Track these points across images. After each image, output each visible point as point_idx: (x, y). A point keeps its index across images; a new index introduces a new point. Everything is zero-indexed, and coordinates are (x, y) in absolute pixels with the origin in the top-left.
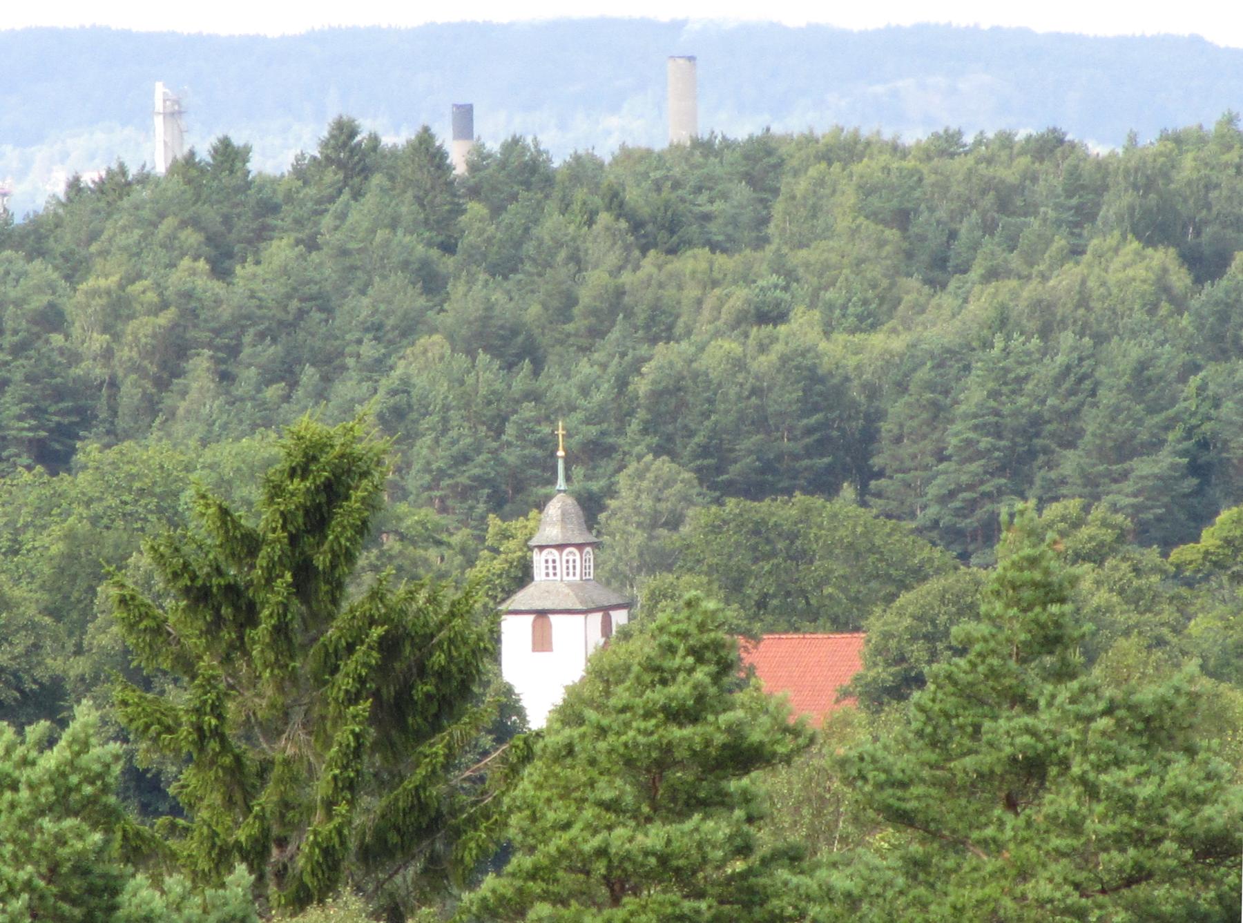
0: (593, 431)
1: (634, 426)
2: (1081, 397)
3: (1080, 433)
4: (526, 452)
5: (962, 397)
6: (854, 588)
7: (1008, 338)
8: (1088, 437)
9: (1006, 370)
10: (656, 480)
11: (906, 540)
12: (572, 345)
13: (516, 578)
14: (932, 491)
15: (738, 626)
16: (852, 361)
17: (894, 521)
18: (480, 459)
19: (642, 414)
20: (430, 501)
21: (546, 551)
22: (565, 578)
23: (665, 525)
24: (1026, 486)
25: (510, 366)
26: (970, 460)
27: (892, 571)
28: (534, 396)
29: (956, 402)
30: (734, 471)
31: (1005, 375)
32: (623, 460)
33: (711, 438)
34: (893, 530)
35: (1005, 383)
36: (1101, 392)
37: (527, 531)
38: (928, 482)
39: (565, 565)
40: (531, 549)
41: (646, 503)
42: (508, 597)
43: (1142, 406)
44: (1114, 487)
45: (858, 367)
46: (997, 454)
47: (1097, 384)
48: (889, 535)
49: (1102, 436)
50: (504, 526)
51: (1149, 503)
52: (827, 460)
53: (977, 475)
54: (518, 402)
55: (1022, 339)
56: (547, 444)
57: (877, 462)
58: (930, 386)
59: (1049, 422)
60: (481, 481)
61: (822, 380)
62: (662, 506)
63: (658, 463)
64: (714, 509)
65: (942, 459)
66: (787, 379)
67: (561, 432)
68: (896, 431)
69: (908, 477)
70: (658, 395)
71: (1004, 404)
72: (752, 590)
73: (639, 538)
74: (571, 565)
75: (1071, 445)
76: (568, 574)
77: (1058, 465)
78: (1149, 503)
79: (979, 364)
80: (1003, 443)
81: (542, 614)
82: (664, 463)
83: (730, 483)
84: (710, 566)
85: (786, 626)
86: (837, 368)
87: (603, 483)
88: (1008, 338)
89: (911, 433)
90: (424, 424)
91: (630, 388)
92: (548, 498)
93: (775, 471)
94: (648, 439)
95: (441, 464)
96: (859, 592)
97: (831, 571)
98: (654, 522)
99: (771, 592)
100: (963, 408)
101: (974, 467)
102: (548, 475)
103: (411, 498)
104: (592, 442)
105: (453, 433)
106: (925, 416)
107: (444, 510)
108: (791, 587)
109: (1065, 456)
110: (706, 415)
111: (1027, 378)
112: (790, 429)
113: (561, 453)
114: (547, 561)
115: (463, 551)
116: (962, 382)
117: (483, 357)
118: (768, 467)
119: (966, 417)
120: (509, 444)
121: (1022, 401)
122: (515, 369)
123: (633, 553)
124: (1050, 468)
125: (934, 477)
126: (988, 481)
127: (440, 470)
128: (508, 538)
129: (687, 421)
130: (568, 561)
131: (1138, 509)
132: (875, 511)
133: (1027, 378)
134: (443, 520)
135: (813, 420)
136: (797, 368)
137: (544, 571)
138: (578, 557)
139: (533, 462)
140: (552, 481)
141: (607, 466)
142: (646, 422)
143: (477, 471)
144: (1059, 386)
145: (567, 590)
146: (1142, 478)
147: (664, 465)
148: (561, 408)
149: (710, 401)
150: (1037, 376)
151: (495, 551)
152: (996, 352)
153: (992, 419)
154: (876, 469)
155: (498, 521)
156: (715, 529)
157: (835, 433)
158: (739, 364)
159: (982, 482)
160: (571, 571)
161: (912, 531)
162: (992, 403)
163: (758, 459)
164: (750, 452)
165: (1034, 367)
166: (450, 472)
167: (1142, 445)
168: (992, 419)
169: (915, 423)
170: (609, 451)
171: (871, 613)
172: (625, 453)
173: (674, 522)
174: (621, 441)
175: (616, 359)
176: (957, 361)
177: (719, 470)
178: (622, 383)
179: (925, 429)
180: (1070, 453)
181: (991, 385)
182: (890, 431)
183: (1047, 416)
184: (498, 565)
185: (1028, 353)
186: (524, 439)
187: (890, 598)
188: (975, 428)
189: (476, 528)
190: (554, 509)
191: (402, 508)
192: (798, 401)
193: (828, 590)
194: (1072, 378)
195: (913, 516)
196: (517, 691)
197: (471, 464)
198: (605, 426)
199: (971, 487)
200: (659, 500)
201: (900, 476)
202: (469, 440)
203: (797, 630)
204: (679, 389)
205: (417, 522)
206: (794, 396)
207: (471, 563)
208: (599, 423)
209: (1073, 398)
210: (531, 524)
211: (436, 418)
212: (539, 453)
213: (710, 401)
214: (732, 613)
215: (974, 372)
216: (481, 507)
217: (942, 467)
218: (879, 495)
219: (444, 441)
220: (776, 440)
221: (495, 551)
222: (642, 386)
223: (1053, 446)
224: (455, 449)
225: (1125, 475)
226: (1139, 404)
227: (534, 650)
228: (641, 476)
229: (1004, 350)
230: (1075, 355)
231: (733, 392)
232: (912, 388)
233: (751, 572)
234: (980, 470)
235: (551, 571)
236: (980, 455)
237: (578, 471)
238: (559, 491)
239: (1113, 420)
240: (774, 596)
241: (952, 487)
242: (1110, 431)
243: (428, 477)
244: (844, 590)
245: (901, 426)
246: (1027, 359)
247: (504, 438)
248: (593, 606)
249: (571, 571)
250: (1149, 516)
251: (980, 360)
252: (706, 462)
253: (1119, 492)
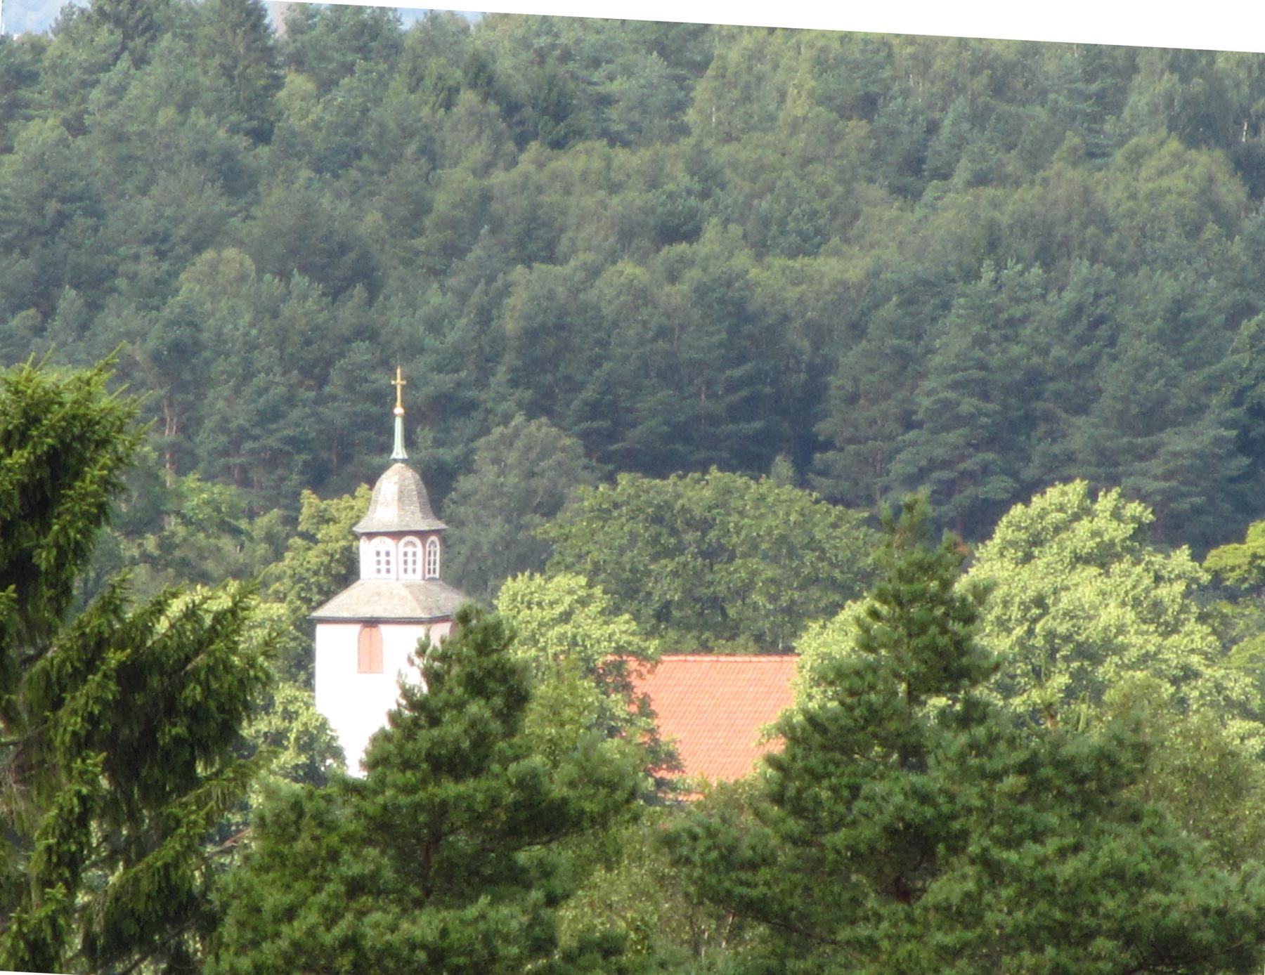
1: (501, 373)
2: (1095, 346)
4: (358, 408)
5: (937, 343)
7: (1000, 266)
8: (1106, 401)
9: (998, 310)
10: (528, 448)
11: (855, 533)
13: (338, 575)
16: (793, 293)
17: (840, 508)
18: (295, 414)
19: (510, 359)
21: (377, 540)
26: (946, 428)
27: (837, 574)
28: (366, 333)
29: (930, 351)
30: (633, 437)
31: (996, 315)
32: (485, 420)
33: (603, 393)
34: (840, 518)
35: (995, 327)
36: (1122, 339)
38: (890, 458)
39: (401, 559)
40: (357, 537)
41: (512, 480)
44: (1138, 466)
46: (984, 420)
47: (1118, 328)
48: (835, 526)
49: (1125, 399)
50: (323, 505)
51: (1184, 489)
52: (757, 425)
53: (957, 447)
55: (1020, 267)
56: (384, 398)
57: (823, 428)
58: (895, 328)
59: (1052, 379)
61: (749, 319)
62: (536, 483)
63: (533, 426)
65: (909, 425)
68: (849, 387)
70: (532, 335)
71: (992, 354)
74: (410, 559)
75: (1082, 410)
77: (1064, 436)
79: (962, 300)
80: (991, 407)
81: (371, 623)
85: (694, 644)
86: (773, 304)
87: (458, 450)
88: (1000, 266)
91: (494, 324)
92: (383, 468)
97: (754, 573)
100: (937, 360)
101: (952, 437)
106: (888, 368)
110: (596, 363)
111: (1025, 318)
112: (709, 383)
113: (399, 410)
115: (270, 538)
117: (300, 281)
119: (945, 370)
120: (334, 398)
121: (1015, 350)
124: (1054, 441)
126: (970, 456)
127: (242, 429)
128: (327, 521)
133: (1025, 318)
135: (737, 372)
140: (388, 448)
141: (463, 427)
143: (289, 432)
144: (1067, 332)
145: (405, 593)
146: (1176, 455)
147: (541, 429)
152: (984, 283)
155: (314, 499)
158: (642, 296)
159: (963, 458)
160: (410, 566)
162: (978, 353)
165: (1035, 306)
166: (257, 431)
167: (1177, 412)
168: (977, 374)
169: (874, 378)
171: (806, 628)
172: (488, 411)
174: (483, 396)
175: (481, 287)
176: (934, 295)
177: (612, 436)
178: (485, 316)
180: (1080, 421)
181: (976, 328)
183: (1049, 370)
184: (314, 557)
188: (955, 386)
189: (286, 507)
192: (721, 345)
194: (1085, 321)
197: (282, 422)
199: (947, 464)
204: (562, 328)
209: (1085, 348)
210: (359, 504)
212: (374, 410)
213: (603, 344)
218: (823, 473)
219: (248, 391)
222: (510, 325)
225: (1153, 452)
226: (1173, 357)
228: (509, 442)
230: (1091, 290)
232: (871, 328)
234: (961, 441)
235: (383, 567)
236: (961, 421)
237: (425, 434)
238: (396, 461)
239: (1139, 378)
241: (924, 463)
242: (1135, 392)
243: (223, 439)
244: (773, 598)
245: (856, 380)
247: (328, 389)
248: (438, 614)
250: (1185, 505)
251: (964, 295)
252: (595, 425)
253: (1144, 474)
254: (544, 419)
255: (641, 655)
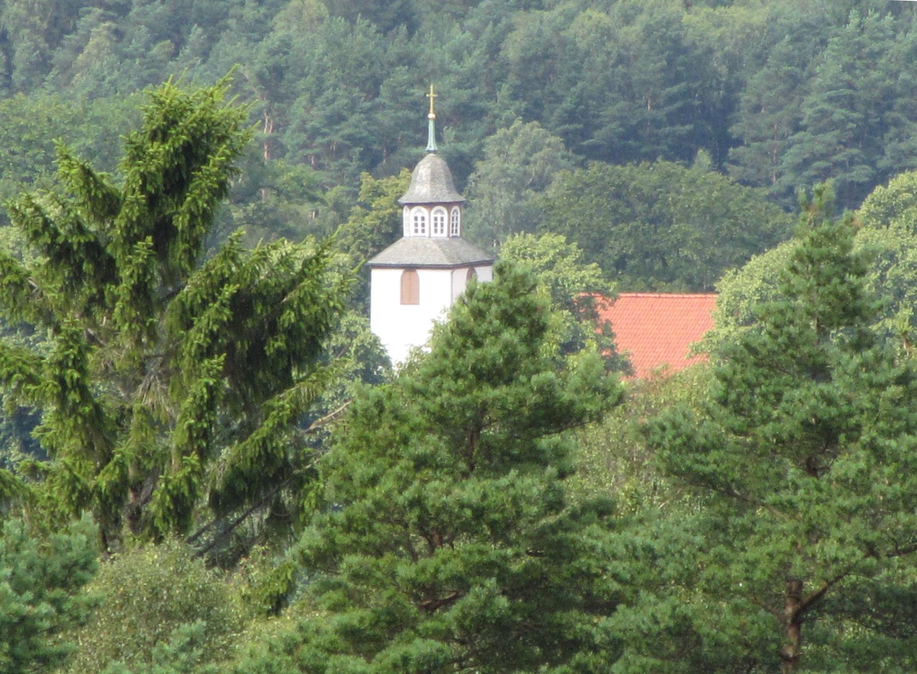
1: (504, 91)
4: (400, 114)
5: (818, 69)
6: (709, 251)
7: (863, 14)
9: (861, 46)
10: (525, 144)
12: (447, 12)
14: (789, 159)
15: (596, 284)
16: (716, 33)
17: (749, 188)
18: (354, 118)
19: (512, 79)
20: (306, 160)
21: (415, 209)
22: (433, 234)
23: (532, 185)
24: (878, 157)
25: (385, 31)
26: (823, 131)
28: (407, 60)
29: (812, 75)
30: (598, 137)
31: (859, 50)
32: (493, 123)
33: (577, 104)
34: (748, 196)
35: (860, 58)
37: (398, 189)
38: (783, 152)
39: (433, 222)
42: (379, 251)
45: (721, 39)
46: (851, 125)
48: (744, 201)
52: (689, 127)
53: (830, 145)
54: (392, 65)
55: (877, 15)
56: (420, 106)
57: (735, 130)
58: (788, 59)
59: (901, 95)
60: (353, 140)
61: (685, 51)
64: (578, 172)
65: (797, 129)
66: (652, 49)
67: (432, 95)
68: (754, 100)
69: (765, 145)
70: (527, 62)
71: (857, 77)
72: (614, 249)
73: (505, 200)
74: (439, 222)
76: (436, 231)
77: (908, 137)
79: (836, 39)
80: (856, 115)
81: (410, 268)
82: (532, 128)
84: (572, 226)
87: (473, 144)
88: (863, 14)
89: (768, 104)
90: (301, 84)
92: (421, 157)
94: (517, 103)
95: (315, 123)
96: (714, 255)
97: (686, 234)
98: (518, 185)
99: (630, 253)
100: (818, 81)
103: (288, 155)
105: (329, 93)
106: (782, 87)
107: (319, 167)
108: (648, 247)
110: (573, 82)
111: (880, 53)
112: (654, 97)
113: (431, 115)
114: (416, 219)
116: (819, 57)
117: (362, 22)
118: (632, 133)
119: (822, 89)
120: (384, 106)
121: (874, 74)
122: (390, 34)
123: (499, 213)
124: (901, 141)
125: (790, 146)
128: (379, 195)
129: (553, 88)
130: (436, 219)
132: (732, 179)
133: (880, 53)
134: (321, 176)
135: (675, 89)
136: (662, 38)
137: (413, 228)
138: (446, 216)
140: (424, 143)
141: (477, 128)
142: (515, 87)
143: (347, 131)
145: (435, 247)
148: (434, 72)
149: (577, 68)
150: (891, 51)
151: (366, 206)
152: (850, 28)
154: (734, 137)
156: (577, 192)
158: (607, 34)
159: (835, 152)
160: (439, 228)
161: (769, 198)
162: (846, 77)
163: (621, 125)
164: (614, 118)
170: (480, 114)
171: (723, 275)
173: (541, 184)
174: (490, 105)
175: (490, 26)
177: (585, 135)
178: (494, 49)
179: (782, 100)
181: (846, 59)
182: (748, 101)
183: (899, 89)
184: (369, 221)
185: (882, 31)
186: (397, 101)
187: (742, 261)
188: (830, 100)
189: (349, 184)
190: (424, 169)
191: (280, 164)
192: (663, 70)
193: (684, 252)
195: (769, 183)
196: (382, 342)
197: (343, 124)
198: (476, 89)
199: (824, 157)
200: (526, 162)
201: (756, 144)
202: (345, 101)
203: (653, 290)
204: (547, 57)
205: (293, 179)
206: (659, 65)
207: (344, 219)
208: (471, 87)
210: (402, 182)
211: (310, 79)
212: (412, 115)
213: (577, 68)
214: (591, 272)
215: (829, 46)
216: (354, 164)
218: (735, 162)
219: (320, 101)
220: (640, 106)
221: (366, 206)
222: (512, 51)
223: (904, 119)
224: (329, 110)
227: (402, 303)
229: (859, 26)
231: (599, 59)
233: (611, 233)
234: (834, 140)
235: (420, 228)
236: (834, 125)
237: (449, 133)
238: (429, 152)
240: (632, 257)
241: (807, 156)
243: (304, 136)
244: (699, 252)
245: (759, 96)
246: (882, 35)
248: (459, 262)
249: (439, 228)
251: (836, 35)
254: (536, 123)
255: (604, 292)
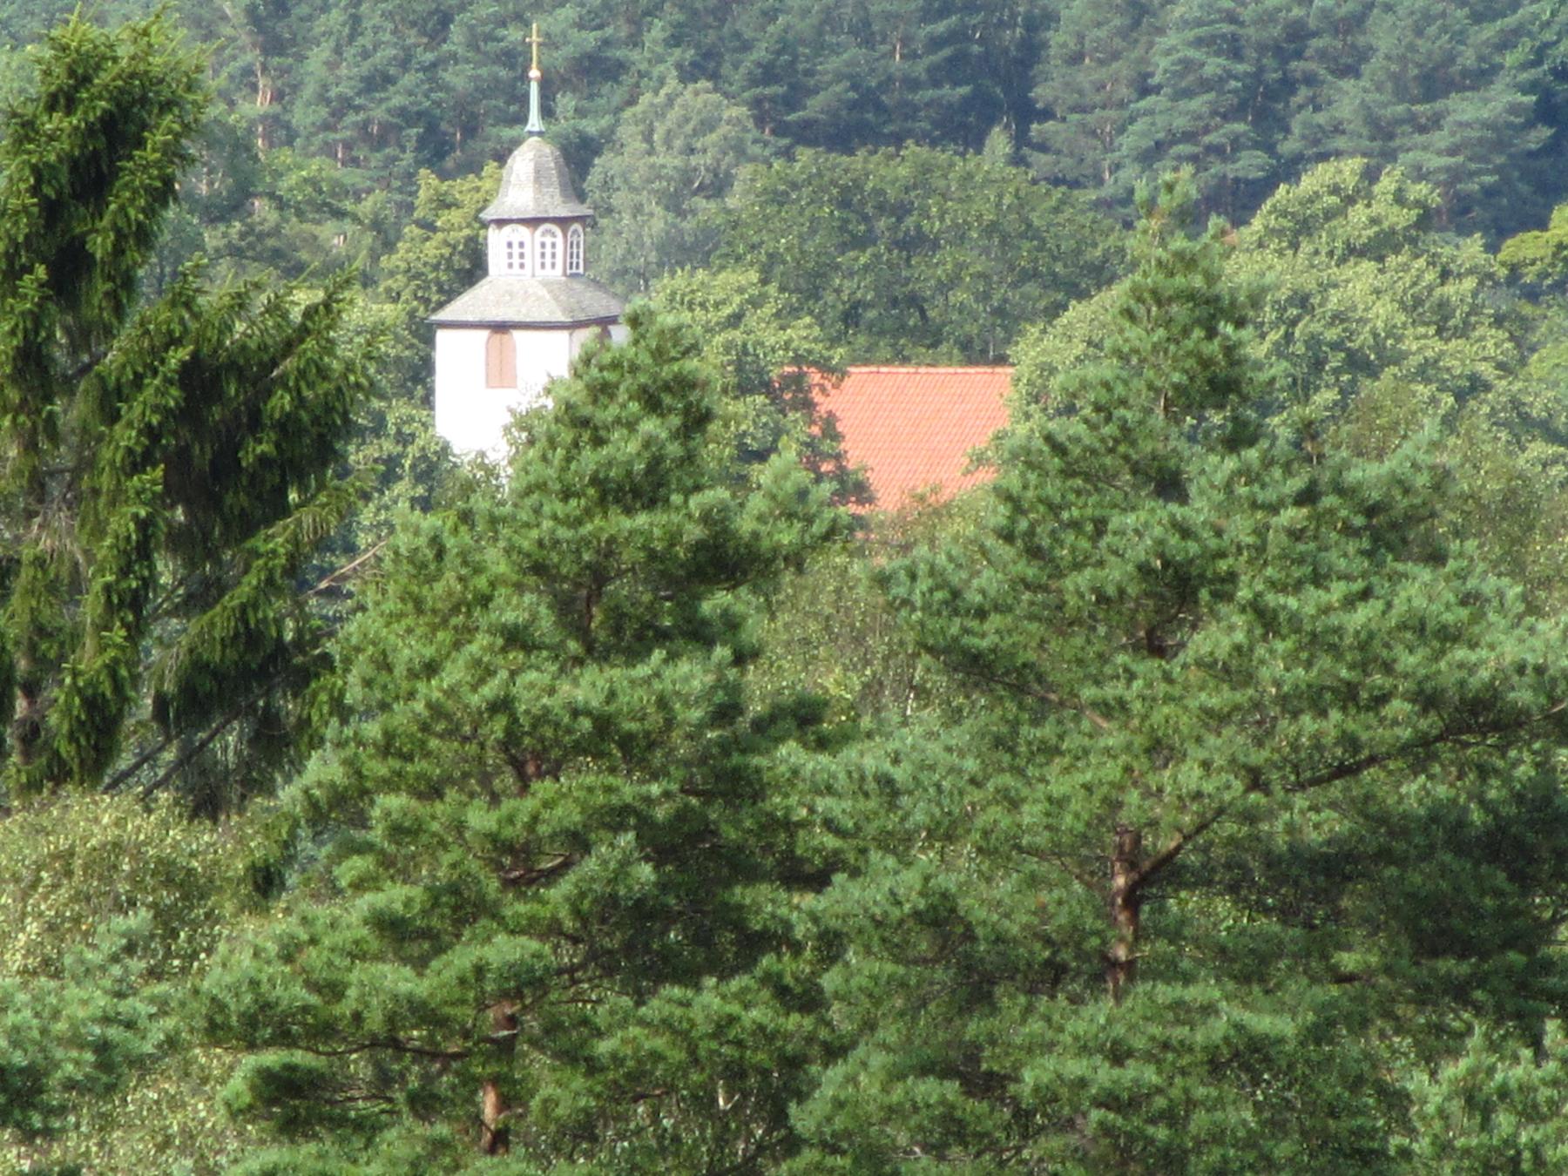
0: (590, 39)
1: (657, 31)
3: (1364, 55)
4: (483, 71)
11: (1080, 219)
14: (1129, 142)
17: (1063, 189)
18: (408, 80)
21: (507, 229)
26: (1188, 94)
30: (814, 107)
33: (779, 53)
34: (1062, 202)
39: (538, 250)
40: (485, 225)
42: (449, 301)
43: (1466, 10)
44: (1419, 138)
46: (1233, 84)
48: (1056, 210)
49: (1402, 59)
50: (444, 187)
51: (1473, 166)
52: (964, 90)
53: (1200, 117)
56: (515, 59)
59: (1314, 34)
60: (407, 116)
64: (777, 165)
65: (1145, 91)
67: (535, 38)
74: (548, 251)
75: (1351, 71)
77: (1330, 103)
78: (1473, 166)
80: (1241, 68)
81: (501, 328)
83: (807, 124)
85: (887, 353)
87: (605, 122)
89: (1096, 50)
92: (516, 142)
93: (879, 108)
94: (677, 52)
95: (345, 89)
96: (1005, 301)
101: (1199, 104)
102: (513, 108)
103: (298, 142)
104: (589, 56)
105: (365, 41)
106: (1117, 21)
109: (1340, 90)
112: (906, 41)
113: (534, 73)
115: (377, 225)
119: (1185, 23)
120: (454, 57)
124: (1317, 109)
125: (1132, 120)
126: (1217, 128)
128: (448, 207)
131: (1456, 175)
132: (1032, 174)
134: (352, 177)
135: (941, 27)
138: (559, 240)
139: (495, 88)
140: (522, 119)
143: (397, 101)
145: (543, 292)
146: (1460, 124)
147: (699, 97)
151: (429, 227)
153: (1226, 28)
154: (1039, 106)
157: (976, 49)
160: (548, 260)
166: (358, 101)
167: (1465, 73)
168: (1226, 28)
169: (1102, 33)
171: (1021, 333)
172: (641, 75)
173: (718, 186)
177: (791, 103)
179: (1118, 43)
180: (1347, 84)
183: (1312, 24)
184: (432, 249)
186: (478, 49)
188: (1199, 42)
189: (400, 190)
190: (523, 162)
191: (285, 156)
193: (959, 296)
196: (456, 451)
198: (609, 31)
200: (692, 151)
201: (1075, 117)
203: (905, 360)
205: (306, 180)
207: (389, 246)
208: (600, 27)
210: (487, 185)
212: (503, 73)
217: (1143, 104)
218: (1043, 148)
221: (429, 227)
225: (1436, 122)
227: (489, 385)
233: (837, 267)
235: (516, 261)
236: (1205, 85)
237: (566, 102)
238: (531, 134)
239: (1419, 32)
241: (1161, 135)
243: (324, 112)
244: (985, 297)
245: (1081, 37)
248: (582, 317)
249: (548, 260)
252: (767, 91)
253: (1425, 148)
255: (825, 366)
